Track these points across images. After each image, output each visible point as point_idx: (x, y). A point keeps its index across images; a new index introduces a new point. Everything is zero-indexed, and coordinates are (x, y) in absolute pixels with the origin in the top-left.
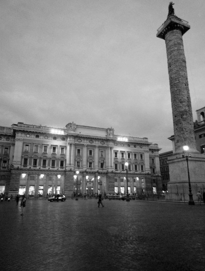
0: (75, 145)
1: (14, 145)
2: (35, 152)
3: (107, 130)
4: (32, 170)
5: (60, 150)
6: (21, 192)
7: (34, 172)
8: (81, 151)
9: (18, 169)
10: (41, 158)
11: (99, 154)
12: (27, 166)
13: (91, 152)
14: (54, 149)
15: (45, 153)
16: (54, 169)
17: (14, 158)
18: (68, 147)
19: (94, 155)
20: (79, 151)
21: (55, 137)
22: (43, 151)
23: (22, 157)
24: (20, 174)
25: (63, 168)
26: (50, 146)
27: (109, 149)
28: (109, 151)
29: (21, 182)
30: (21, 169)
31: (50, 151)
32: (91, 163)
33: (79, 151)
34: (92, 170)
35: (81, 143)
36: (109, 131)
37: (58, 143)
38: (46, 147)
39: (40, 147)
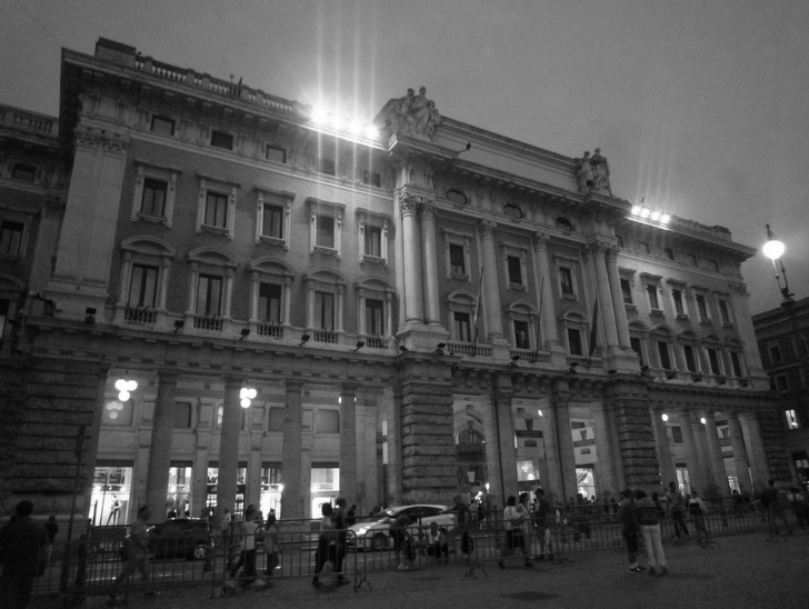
0: (442, 219)
1: (58, 208)
2: (206, 232)
3: (575, 167)
4: (189, 346)
5: (361, 237)
6: (106, 503)
7: (201, 357)
8: (467, 257)
9: (86, 329)
10: (248, 272)
11: (553, 281)
12: (151, 316)
13: (514, 264)
14: (327, 225)
15: (272, 243)
16: (331, 346)
17: (58, 262)
18: (406, 226)
19: (532, 285)
20: (457, 252)
21: (334, 159)
22: (260, 232)
23: (119, 253)
24: (101, 375)
25: (380, 344)
26: (298, 205)
27: (601, 257)
28: (602, 263)
29: (106, 443)
30: (111, 336)
31: (300, 239)
32: (521, 326)
33: (457, 252)
34: (539, 365)
35: (467, 212)
36: (587, 166)
37: (352, 196)
38: (275, 212)
39: (239, 206)
